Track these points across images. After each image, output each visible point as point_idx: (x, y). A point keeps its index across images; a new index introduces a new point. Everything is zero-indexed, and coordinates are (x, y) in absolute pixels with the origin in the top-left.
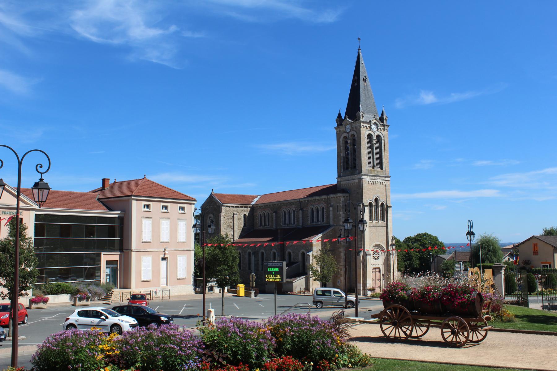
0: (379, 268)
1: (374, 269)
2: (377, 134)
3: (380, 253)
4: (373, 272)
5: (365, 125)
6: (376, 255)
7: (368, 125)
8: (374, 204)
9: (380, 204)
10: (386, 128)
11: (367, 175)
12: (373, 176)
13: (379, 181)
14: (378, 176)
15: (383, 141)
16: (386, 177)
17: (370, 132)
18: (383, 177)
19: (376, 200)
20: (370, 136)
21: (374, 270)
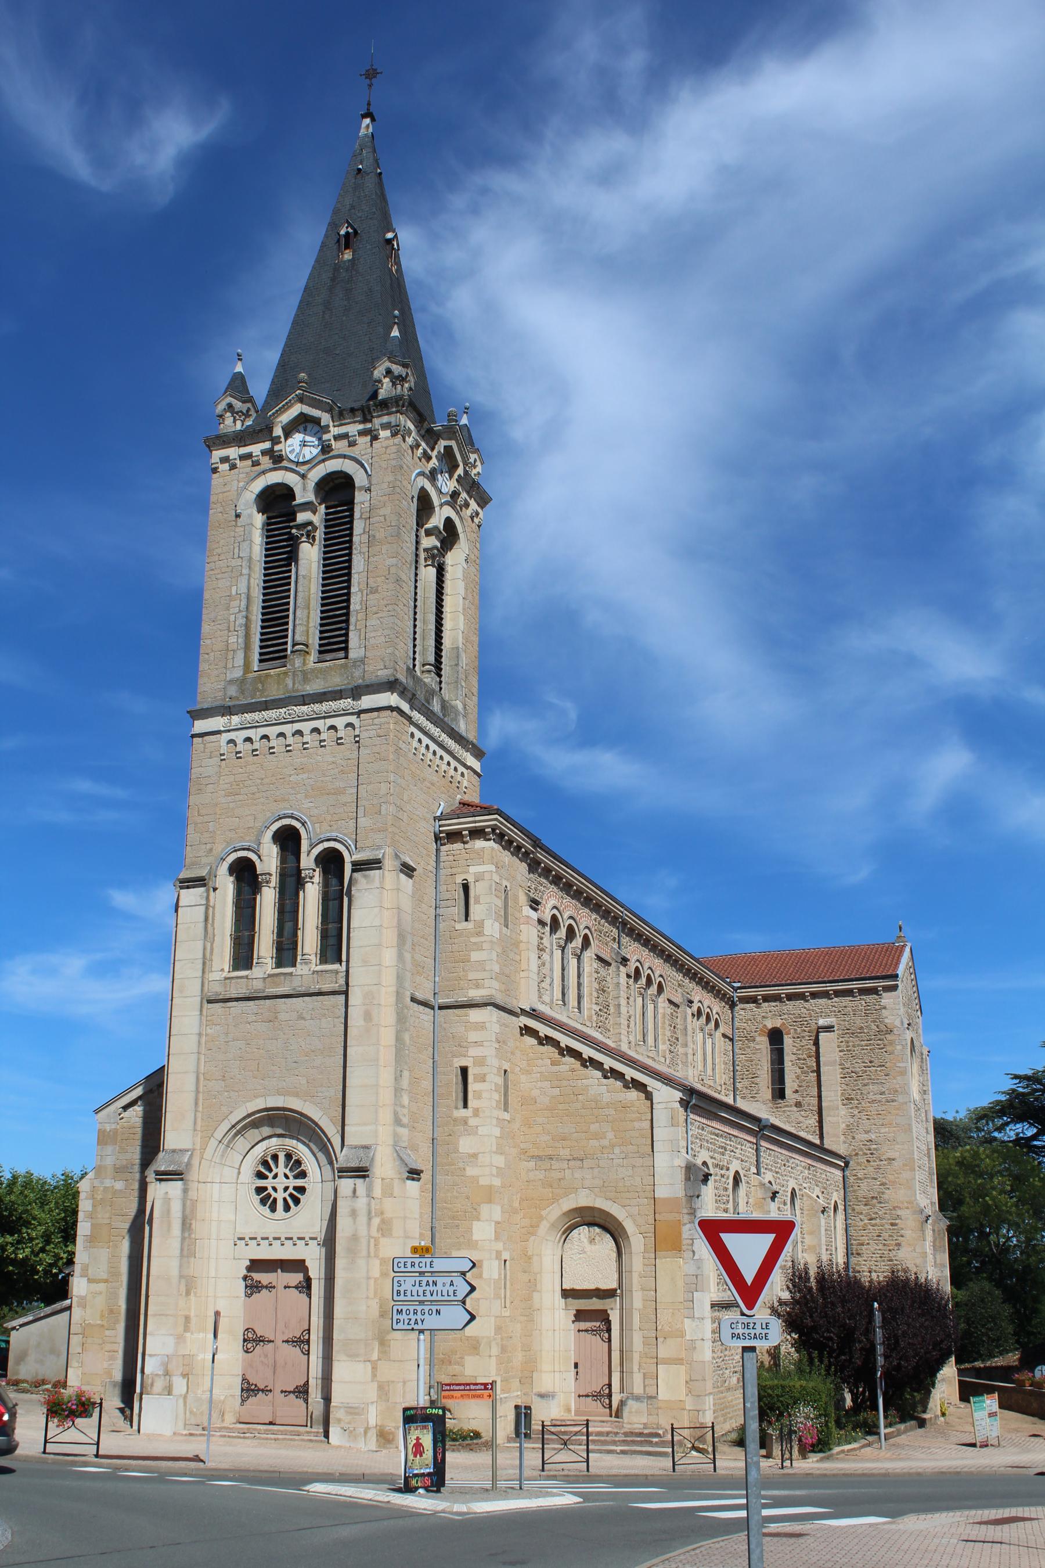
0: (298, 1265)
1: (256, 1265)
2: (317, 474)
3: (310, 1163)
4: (253, 1288)
5: (233, 452)
6: (281, 1182)
7: (256, 449)
8: (269, 860)
9: (307, 861)
10: (377, 422)
11: (227, 711)
12: (266, 706)
13: (306, 727)
14: (305, 700)
15: (359, 497)
16: (356, 693)
17: (276, 477)
18: (337, 695)
19: (288, 840)
20: (277, 503)
21: (264, 1278)
